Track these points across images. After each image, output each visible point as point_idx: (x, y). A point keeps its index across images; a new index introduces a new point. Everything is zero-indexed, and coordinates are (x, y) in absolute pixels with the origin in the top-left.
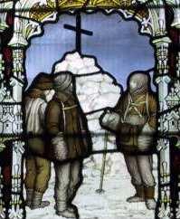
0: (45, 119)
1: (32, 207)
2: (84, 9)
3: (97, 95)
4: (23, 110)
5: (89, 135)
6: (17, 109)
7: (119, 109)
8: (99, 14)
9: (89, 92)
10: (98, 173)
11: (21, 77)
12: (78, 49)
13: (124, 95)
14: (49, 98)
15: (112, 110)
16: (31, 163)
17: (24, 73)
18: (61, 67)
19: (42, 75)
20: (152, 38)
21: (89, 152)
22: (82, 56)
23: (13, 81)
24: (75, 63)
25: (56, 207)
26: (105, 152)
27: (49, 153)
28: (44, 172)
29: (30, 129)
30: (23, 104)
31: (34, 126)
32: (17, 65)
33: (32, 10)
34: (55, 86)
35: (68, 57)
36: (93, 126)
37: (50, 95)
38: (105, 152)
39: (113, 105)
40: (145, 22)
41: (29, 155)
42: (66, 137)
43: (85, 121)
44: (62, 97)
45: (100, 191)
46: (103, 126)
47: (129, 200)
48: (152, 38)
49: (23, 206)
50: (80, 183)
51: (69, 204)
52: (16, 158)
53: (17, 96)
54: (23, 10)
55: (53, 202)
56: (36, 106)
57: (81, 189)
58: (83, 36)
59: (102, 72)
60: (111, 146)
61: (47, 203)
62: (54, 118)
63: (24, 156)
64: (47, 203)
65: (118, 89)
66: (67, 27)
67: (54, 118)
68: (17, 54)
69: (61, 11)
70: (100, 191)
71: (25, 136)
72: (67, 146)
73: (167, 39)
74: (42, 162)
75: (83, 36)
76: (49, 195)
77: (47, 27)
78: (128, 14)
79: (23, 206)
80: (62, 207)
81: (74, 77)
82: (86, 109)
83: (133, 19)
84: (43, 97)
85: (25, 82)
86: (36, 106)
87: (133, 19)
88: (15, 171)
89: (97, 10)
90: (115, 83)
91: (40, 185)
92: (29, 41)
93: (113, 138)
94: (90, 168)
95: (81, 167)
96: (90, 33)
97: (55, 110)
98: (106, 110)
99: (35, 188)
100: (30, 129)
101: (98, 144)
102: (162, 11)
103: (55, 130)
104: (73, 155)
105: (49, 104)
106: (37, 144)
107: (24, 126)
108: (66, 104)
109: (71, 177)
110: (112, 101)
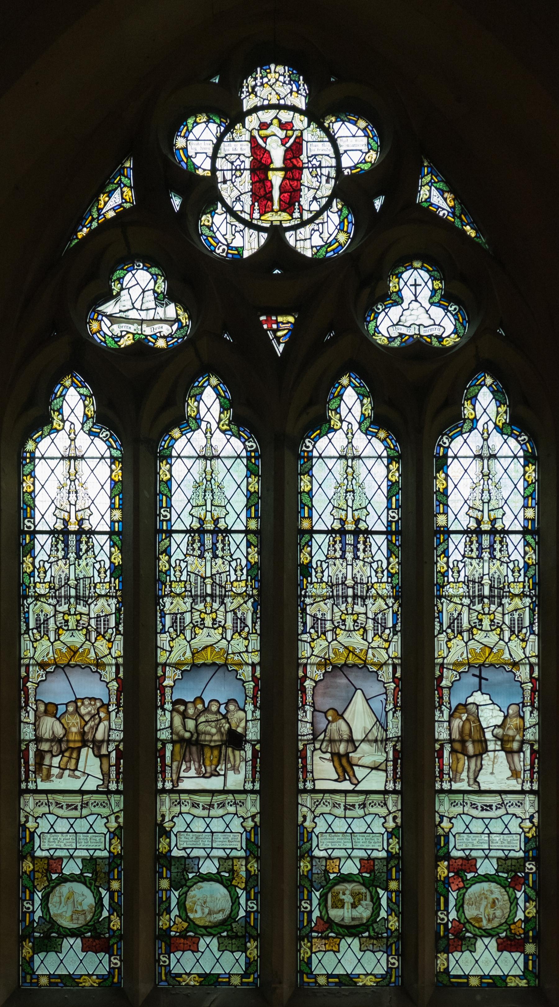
0: (461, 732)
1: (455, 782)
2: (483, 665)
3: (490, 717)
4: (449, 725)
5: (486, 741)
6: (446, 724)
7: (502, 726)
8: (492, 668)
9: (485, 715)
10: (491, 763)
11: (448, 706)
12: (480, 689)
13: (505, 717)
14: (464, 718)
15: (499, 726)
16: (454, 756)
17: (450, 703)
18: (470, 700)
19: (460, 704)
20: (522, 684)
21: (486, 751)
22: (483, 694)
23: (444, 707)
24: (478, 698)
25: (468, 782)
26: (495, 751)
27: (464, 752)
28: (461, 763)
29: (453, 737)
30: (449, 722)
31: (456, 735)
32: (446, 698)
33: (454, 664)
34: (467, 712)
35: (475, 694)
36: (489, 736)
37: (464, 717)
38: (495, 751)
39: (499, 723)
40: (518, 674)
41: (453, 751)
42: (474, 742)
43: (484, 733)
44: (471, 717)
45: (492, 773)
46: (494, 736)
47: (508, 779)
48: (522, 684)
49: (450, 781)
50: (481, 769)
51: (475, 781)
52: (446, 754)
53: (446, 717)
54: (448, 664)
55: (466, 780)
56: (457, 723)
57: (482, 771)
58: (483, 681)
59: (493, 703)
60: (498, 748)
61: (463, 780)
62: (467, 731)
63: (450, 752)
64: (463, 780)
65: (502, 714)
66: (474, 675)
67: (467, 731)
68: (445, 691)
69: (470, 665)
70: (492, 773)
71: (451, 741)
72: (474, 747)
73: (530, 684)
74: (460, 756)
75: (483, 681)
76: (464, 775)
77: (462, 675)
78: (508, 668)
79: (450, 781)
80: (472, 782)
81: (478, 706)
82: (484, 726)
83: (511, 671)
84: (461, 718)
85: (450, 709)
86: (457, 723)
87: (511, 671)
88: (446, 761)
89: (492, 665)
90: (501, 710)
91: (460, 770)
92: (452, 683)
93: (499, 743)
94: (487, 759)
95: (482, 759)
96: (487, 680)
97: (467, 726)
98: (495, 726)
99: (457, 771)
100: (453, 737)
101: (491, 746)
102: (528, 667)
103: (467, 738)
104: (477, 753)
105: (464, 722)
106: (458, 746)
107: (450, 735)
108: (474, 722)
109: (476, 765)
110: (499, 721)
